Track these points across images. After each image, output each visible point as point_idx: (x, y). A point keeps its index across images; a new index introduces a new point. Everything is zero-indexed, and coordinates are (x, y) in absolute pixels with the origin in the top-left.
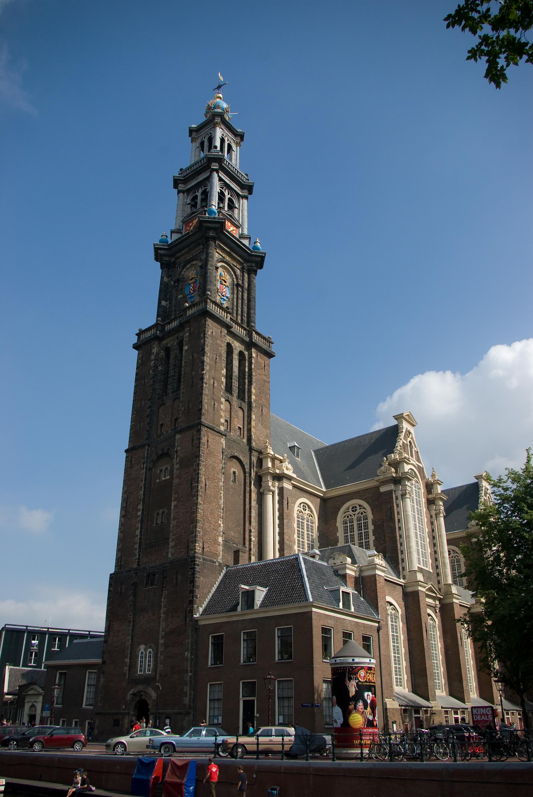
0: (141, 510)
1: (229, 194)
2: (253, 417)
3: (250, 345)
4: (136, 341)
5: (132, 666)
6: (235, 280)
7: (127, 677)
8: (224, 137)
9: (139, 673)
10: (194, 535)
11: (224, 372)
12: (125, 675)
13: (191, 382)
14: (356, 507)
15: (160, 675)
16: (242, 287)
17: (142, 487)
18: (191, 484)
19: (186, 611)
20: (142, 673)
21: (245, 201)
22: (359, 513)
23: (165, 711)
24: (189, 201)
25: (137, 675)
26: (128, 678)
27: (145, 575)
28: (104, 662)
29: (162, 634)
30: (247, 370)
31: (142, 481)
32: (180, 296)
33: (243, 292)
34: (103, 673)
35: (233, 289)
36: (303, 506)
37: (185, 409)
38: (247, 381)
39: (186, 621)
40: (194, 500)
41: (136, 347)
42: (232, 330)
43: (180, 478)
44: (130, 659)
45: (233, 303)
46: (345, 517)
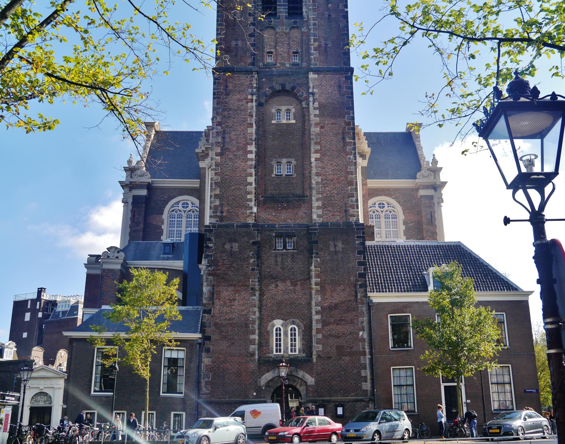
0: (254, 152)
5: (264, 343)
7: (257, 357)
9: (275, 353)
10: (354, 199)
12: (253, 354)
13: (327, 16)
15: (319, 356)
17: (252, 124)
18: (344, 138)
19: (355, 286)
20: (282, 353)
23: (332, 398)
25: (273, 356)
26: (259, 360)
27: (274, 235)
28: (206, 338)
29: (314, 309)
31: (252, 116)
34: (208, 351)
37: (320, 46)
39: (356, 296)
40: (350, 158)
43: (322, 127)
44: (259, 336)
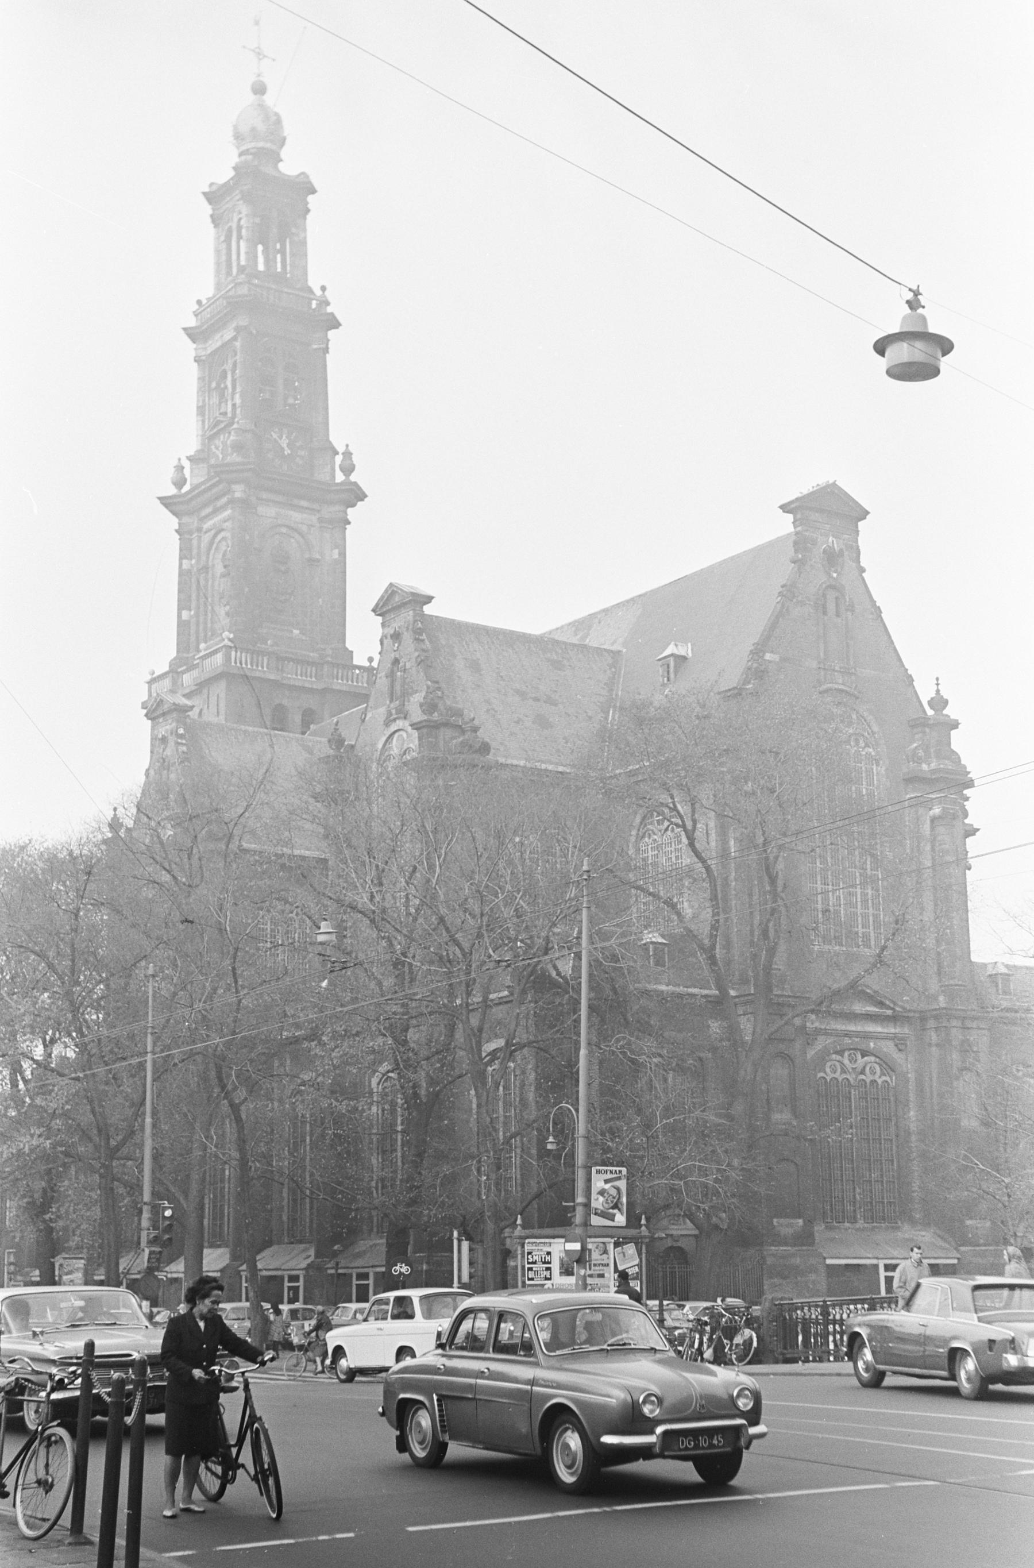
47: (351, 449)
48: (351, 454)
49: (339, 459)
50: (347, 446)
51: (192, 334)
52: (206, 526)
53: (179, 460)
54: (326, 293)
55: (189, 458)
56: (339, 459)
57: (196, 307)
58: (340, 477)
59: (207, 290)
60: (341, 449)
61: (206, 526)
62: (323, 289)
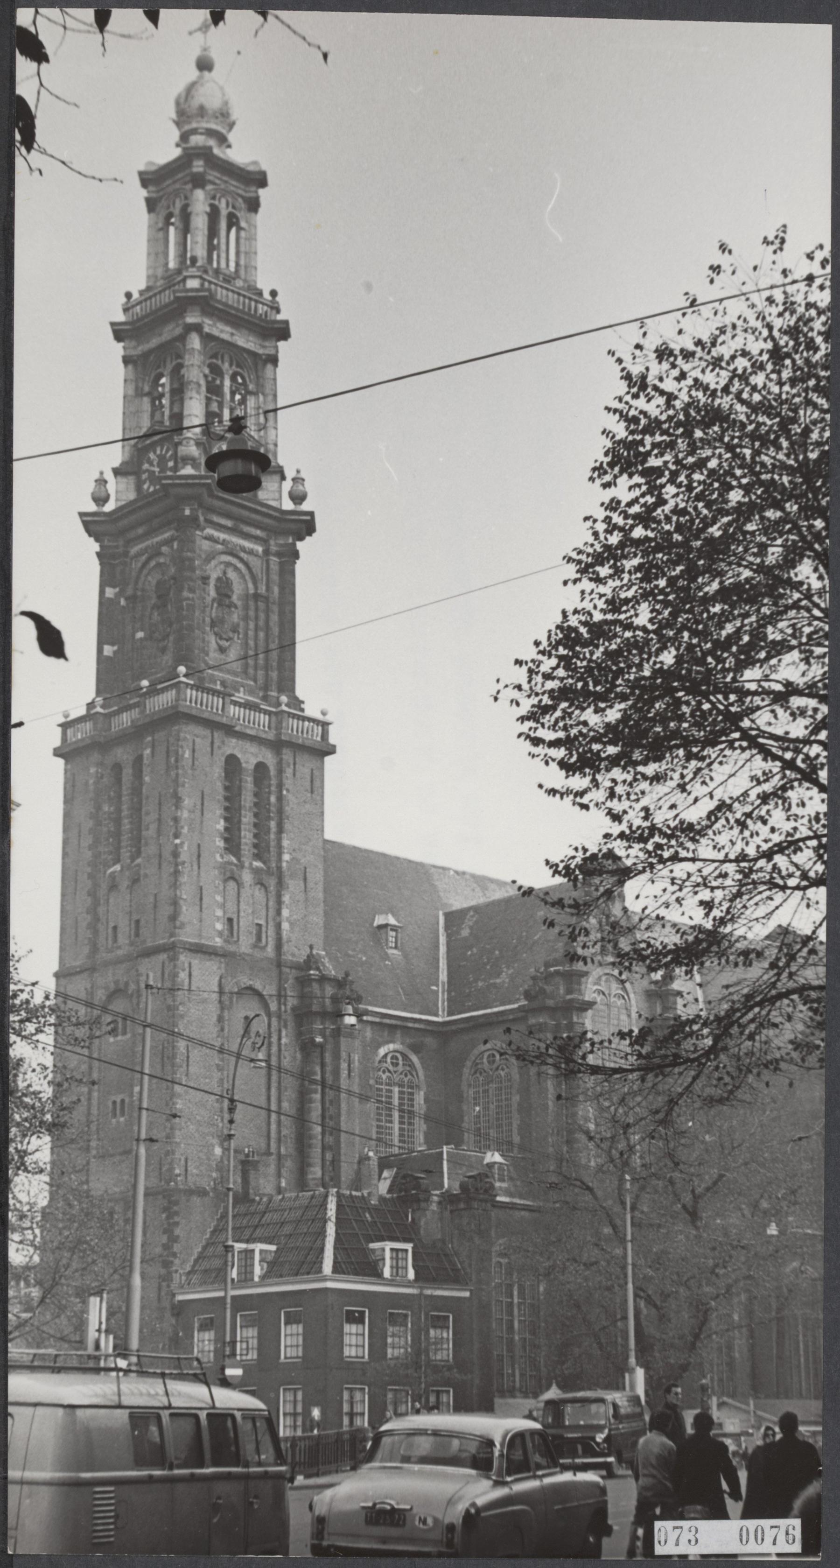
1: (231, 365)
2: (286, 898)
3: (278, 745)
4: (57, 743)
6: (251, 585)
8: (216, 203)
11: (221, 825)
14: (494, 1056)
16: (266, 599)
21: (269, 367)
22: (497, 1069)
24: (147, 389)
30: (273, 799)
32: (140, 635)
33: (267, 611)
35: (246, 608)
36: (392, 1058)
38: (273, 824)
41: (57, 753)
42: (237, 728)
45: (247, 644)
46: (475, 1073)
47: (303, 475)
48: (303, 480)
49: (287, 485)
50: (298, 472)
51: (119, 333)
52: (134, 550)
53: (102, 473)
54: (278, 299)
55: (117, 472)
56: (287, 485)
57: (124, 300)
58: (287, 505)
59: (138, 283)
60: (290, 474)
61: (134, 550)
62: (274, 293)
